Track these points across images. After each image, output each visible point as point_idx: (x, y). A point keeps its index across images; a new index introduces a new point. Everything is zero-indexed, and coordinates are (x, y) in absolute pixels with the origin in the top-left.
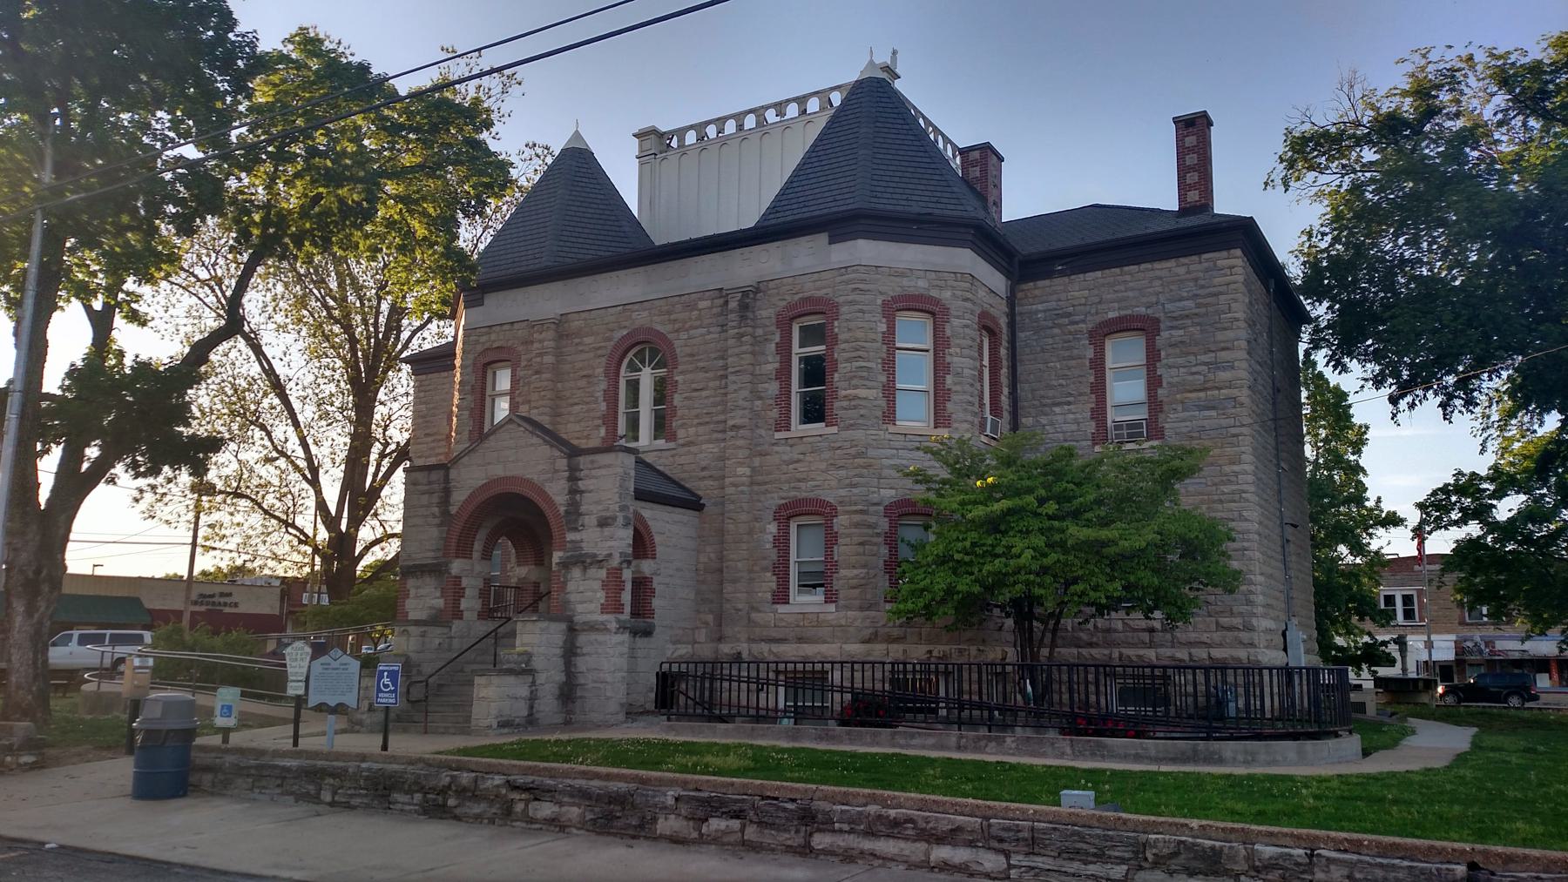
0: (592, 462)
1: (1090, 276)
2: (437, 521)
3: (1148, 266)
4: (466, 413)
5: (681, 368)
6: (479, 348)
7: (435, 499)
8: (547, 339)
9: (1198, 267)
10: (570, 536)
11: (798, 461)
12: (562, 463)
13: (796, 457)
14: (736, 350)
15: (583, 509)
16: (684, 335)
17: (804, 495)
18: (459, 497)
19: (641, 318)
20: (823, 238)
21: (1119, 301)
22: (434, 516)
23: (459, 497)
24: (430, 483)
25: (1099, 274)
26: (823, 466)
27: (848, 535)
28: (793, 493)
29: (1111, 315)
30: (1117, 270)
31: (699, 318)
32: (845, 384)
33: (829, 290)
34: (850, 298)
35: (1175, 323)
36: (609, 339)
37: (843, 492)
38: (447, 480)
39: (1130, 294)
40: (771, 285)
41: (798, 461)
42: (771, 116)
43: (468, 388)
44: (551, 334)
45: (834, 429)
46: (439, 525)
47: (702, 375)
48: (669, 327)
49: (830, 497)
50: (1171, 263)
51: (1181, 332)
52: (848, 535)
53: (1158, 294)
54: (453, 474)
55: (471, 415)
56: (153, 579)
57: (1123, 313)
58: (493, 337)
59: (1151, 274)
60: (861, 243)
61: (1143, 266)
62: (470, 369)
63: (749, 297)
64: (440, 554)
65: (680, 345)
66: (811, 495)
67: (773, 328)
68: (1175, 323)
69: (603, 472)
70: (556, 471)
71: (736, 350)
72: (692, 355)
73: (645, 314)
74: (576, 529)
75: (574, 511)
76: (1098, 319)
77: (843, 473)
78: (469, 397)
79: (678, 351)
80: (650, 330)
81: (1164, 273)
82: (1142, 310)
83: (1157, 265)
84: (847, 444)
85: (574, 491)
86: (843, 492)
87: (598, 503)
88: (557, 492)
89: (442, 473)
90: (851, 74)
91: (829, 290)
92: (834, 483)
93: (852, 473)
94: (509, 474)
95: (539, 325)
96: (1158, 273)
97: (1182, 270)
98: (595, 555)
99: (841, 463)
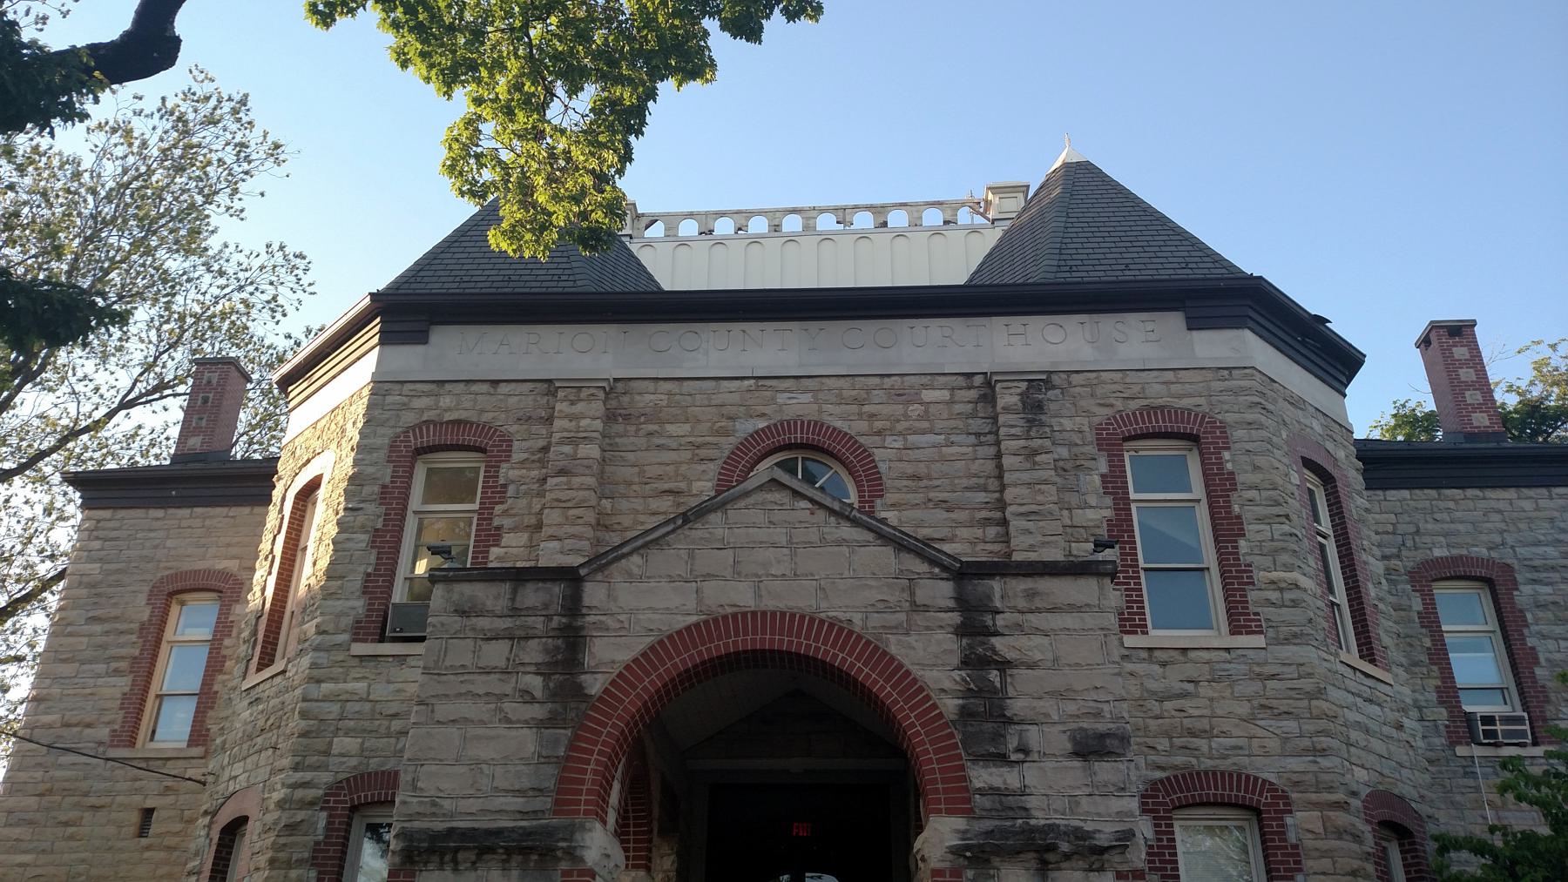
0: (1031, 595)
1: (1393, 495)
2: (538, 712)
3: (1477, 492)
4: (363, 538)
5: (890, 497)
6: (409, 418)
7: (533, 652)
8: (590, 414)
9: (1551, 504)
10: (982, 776)
11: (1184, 695)
12: (941, 591)
13: (1178, 687)
14: (1026, 476)
15: (1017, 706)
16: (895, 443)
17: (1208, 764)
18: (608, 655)
19: (798, 405)
20: (1174, 321)
21: (1446, 535)
22: (527, 697)
23: (608, 655)
24: (514, 612)
25: (1406, 493)
26: (1243, 709)
27: (1325, 854)
28: (1179, 760)
29: (1437, 553)
30: (1433, 493)
31: (925, 416)
32: (1267, 562)
33: (1201, 401)
34: (1250, 417)
35: (1536, 576)
36: (725, 433)
37: (1295, 764)
38: (574, 606)
39: (1461, 527)
40: (1076, 378)
41: (1184, 695)
42: (826, 223)
43: (372, 489)
44: (597, 407)
45: (1258, 641)
46: (540, 724)
47: (941, 514)
48: (862, 426)
49: (1269, 770)
50: (1511, 493)
51: (1548, 589)
52: (1325, 854)
53: (1501, 532)
54: (593, 593)
55: (373, 544)
56: (994, 249)
57: (1455, 552)
58: (446, 401)
59: (1482, 504)
60: (1248, 335)
61: (1470, 492)
62: (381, 455)
63: (1038, 391)
64: (544, 803)
65: (885, 455)
66: (1225, 765)
67: (1091, 449)
68: (1536, 576)
69: (1069, 620)
70: (916, 608)
71: (1026, 476)
72: (916, 477)
73: (807, 397)
74: (1002, 759)
75: (987, 720)
76: (1420, 556)
77: (1290, 725)
78: (371, 508)
79: (883, 467)
80: (819, 426)
81: (1501, 505)
82: (1484, 552)
83: (1490, 493)
84: (1291, 671)
85: (976, 662)
86: (1295, 764)
87: (1061, 695)
88: (930, 658)
89: (558, 589)
90: (1036, 168)
91: (1201, 401)
92: (1273, 744)
93: (1309, 727)
94: (769, 604)
95: (577, 387)
96: (1493, 504)
97: (1528, 505)
98: (1079, 835)
99: (1283, 706)
